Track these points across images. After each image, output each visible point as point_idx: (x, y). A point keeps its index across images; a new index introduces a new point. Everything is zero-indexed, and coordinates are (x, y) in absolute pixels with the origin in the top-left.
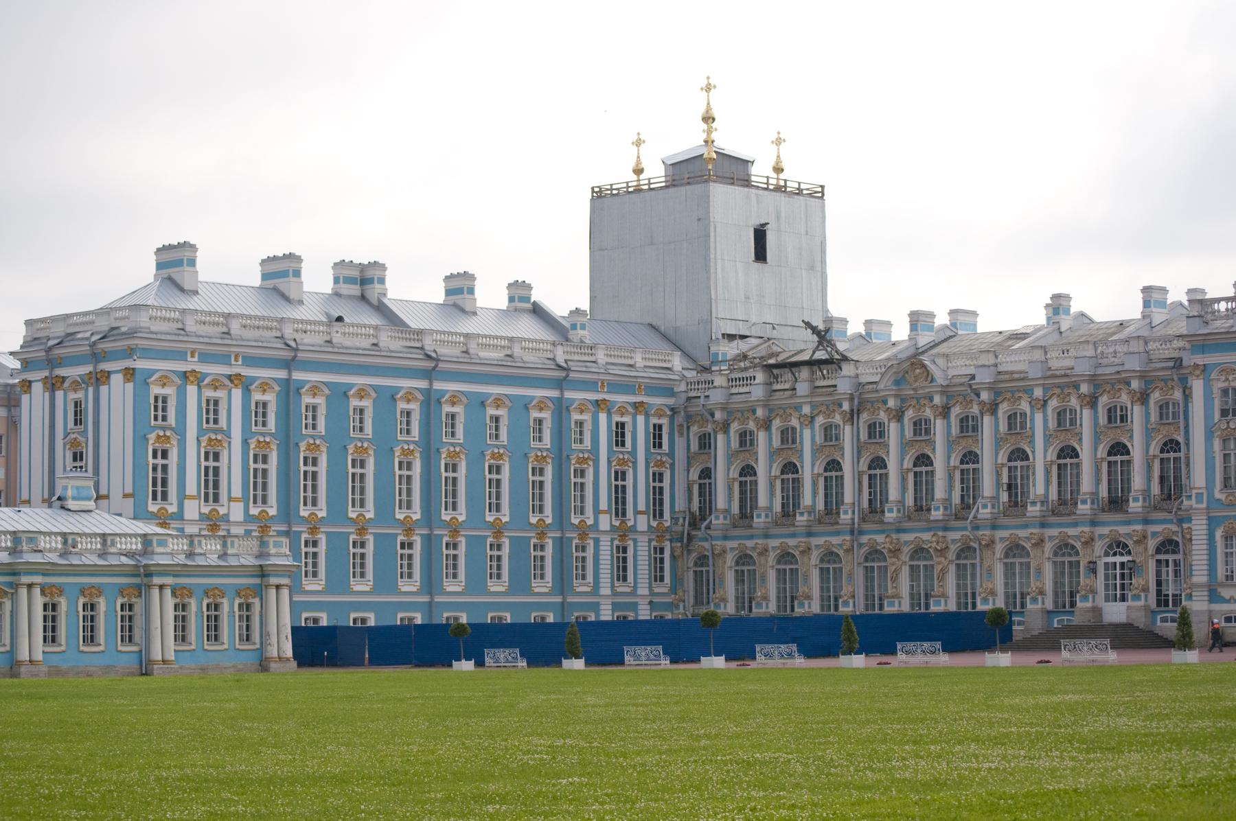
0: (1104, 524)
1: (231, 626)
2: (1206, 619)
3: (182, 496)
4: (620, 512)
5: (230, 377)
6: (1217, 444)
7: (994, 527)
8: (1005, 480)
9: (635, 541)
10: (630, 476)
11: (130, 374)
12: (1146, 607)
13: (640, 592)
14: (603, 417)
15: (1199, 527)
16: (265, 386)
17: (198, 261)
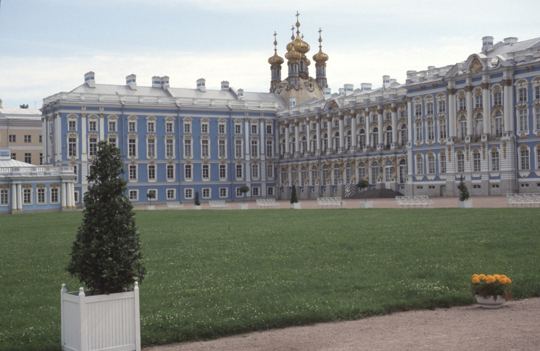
0: (358, 156)
1: (48, 197)
2: (411, 187)
3: (81, 153)
4: (269, 154)
5: (99, 115)
6: (415, 125)
7: (355, 156)
8: (359, 140)
9: (260, 164)
10: (258, 142)
11: (60, 114)
12: (396, 184)
13: (262, 180)
14: (247, 124)
15: (409, 154)
16: (113, 117)
17: (95, 78)
